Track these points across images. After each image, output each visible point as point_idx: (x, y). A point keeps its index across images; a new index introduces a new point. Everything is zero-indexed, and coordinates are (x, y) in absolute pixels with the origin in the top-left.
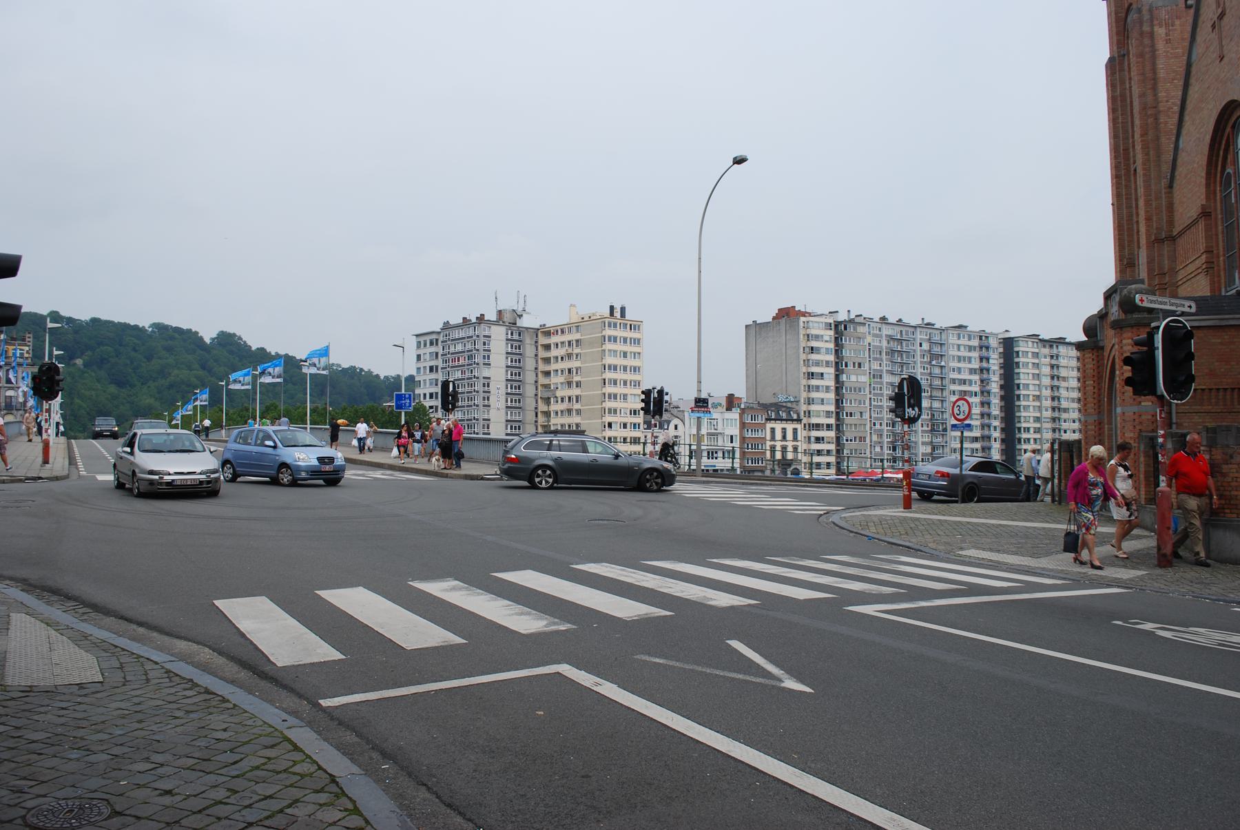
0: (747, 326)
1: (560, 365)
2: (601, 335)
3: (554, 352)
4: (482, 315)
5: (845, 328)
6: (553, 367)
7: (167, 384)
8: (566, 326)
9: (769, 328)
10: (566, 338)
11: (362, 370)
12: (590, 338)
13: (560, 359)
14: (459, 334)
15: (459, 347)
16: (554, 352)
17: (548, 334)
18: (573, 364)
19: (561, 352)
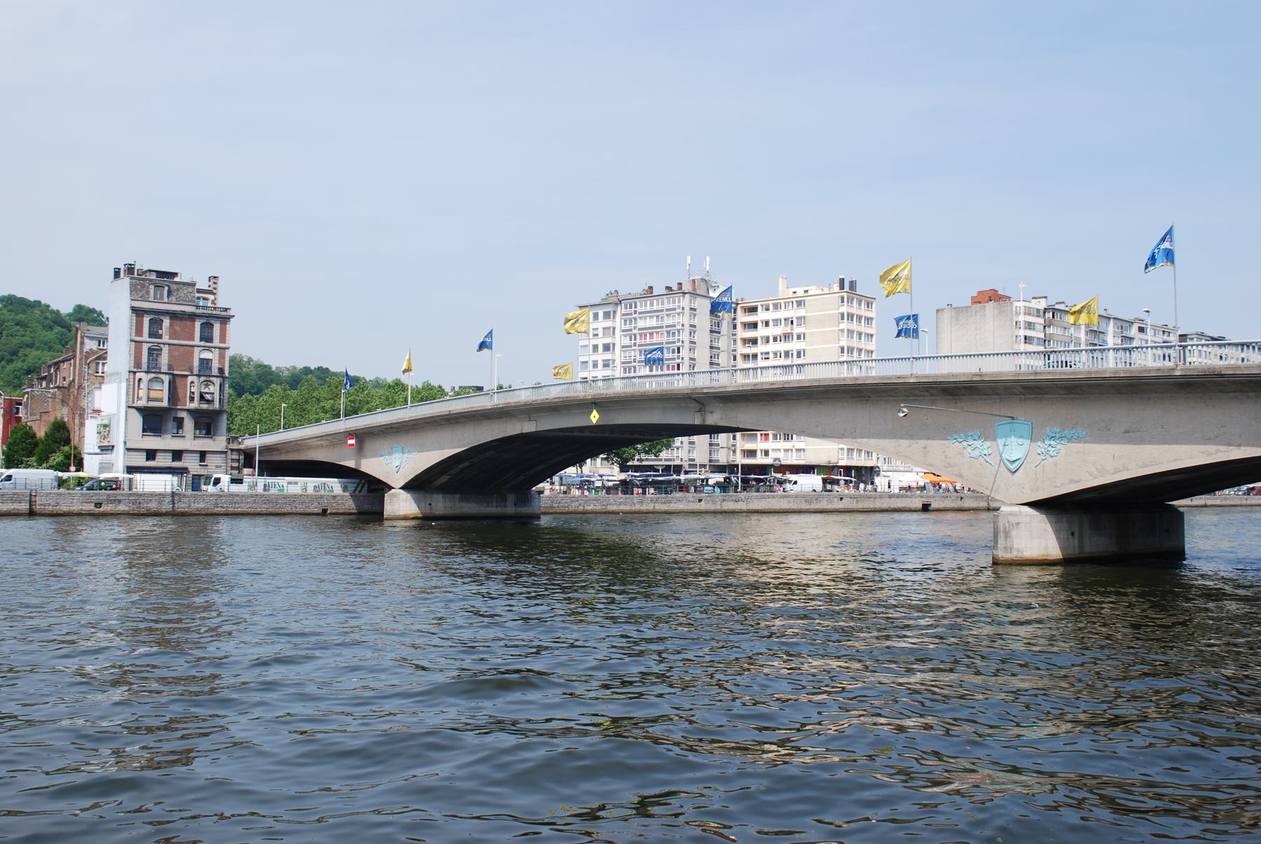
0: (937, 311)
1: (772, 347)
2: (837, 312)
3: (761, 332)
4: (651, 288)
5: (1053, 317)
6: (759, 349)
7: (25, 367)
8: (782, 301)
9: (969, 313)
10: (782, 314)
11: (250, 360)
12: (820, 315)
13: (771, 339)
14: (652, 305)
15: (652, 322)
16: (761, 332)
17: (753, 310)
18: (794, 346)
19: (778, 331)
